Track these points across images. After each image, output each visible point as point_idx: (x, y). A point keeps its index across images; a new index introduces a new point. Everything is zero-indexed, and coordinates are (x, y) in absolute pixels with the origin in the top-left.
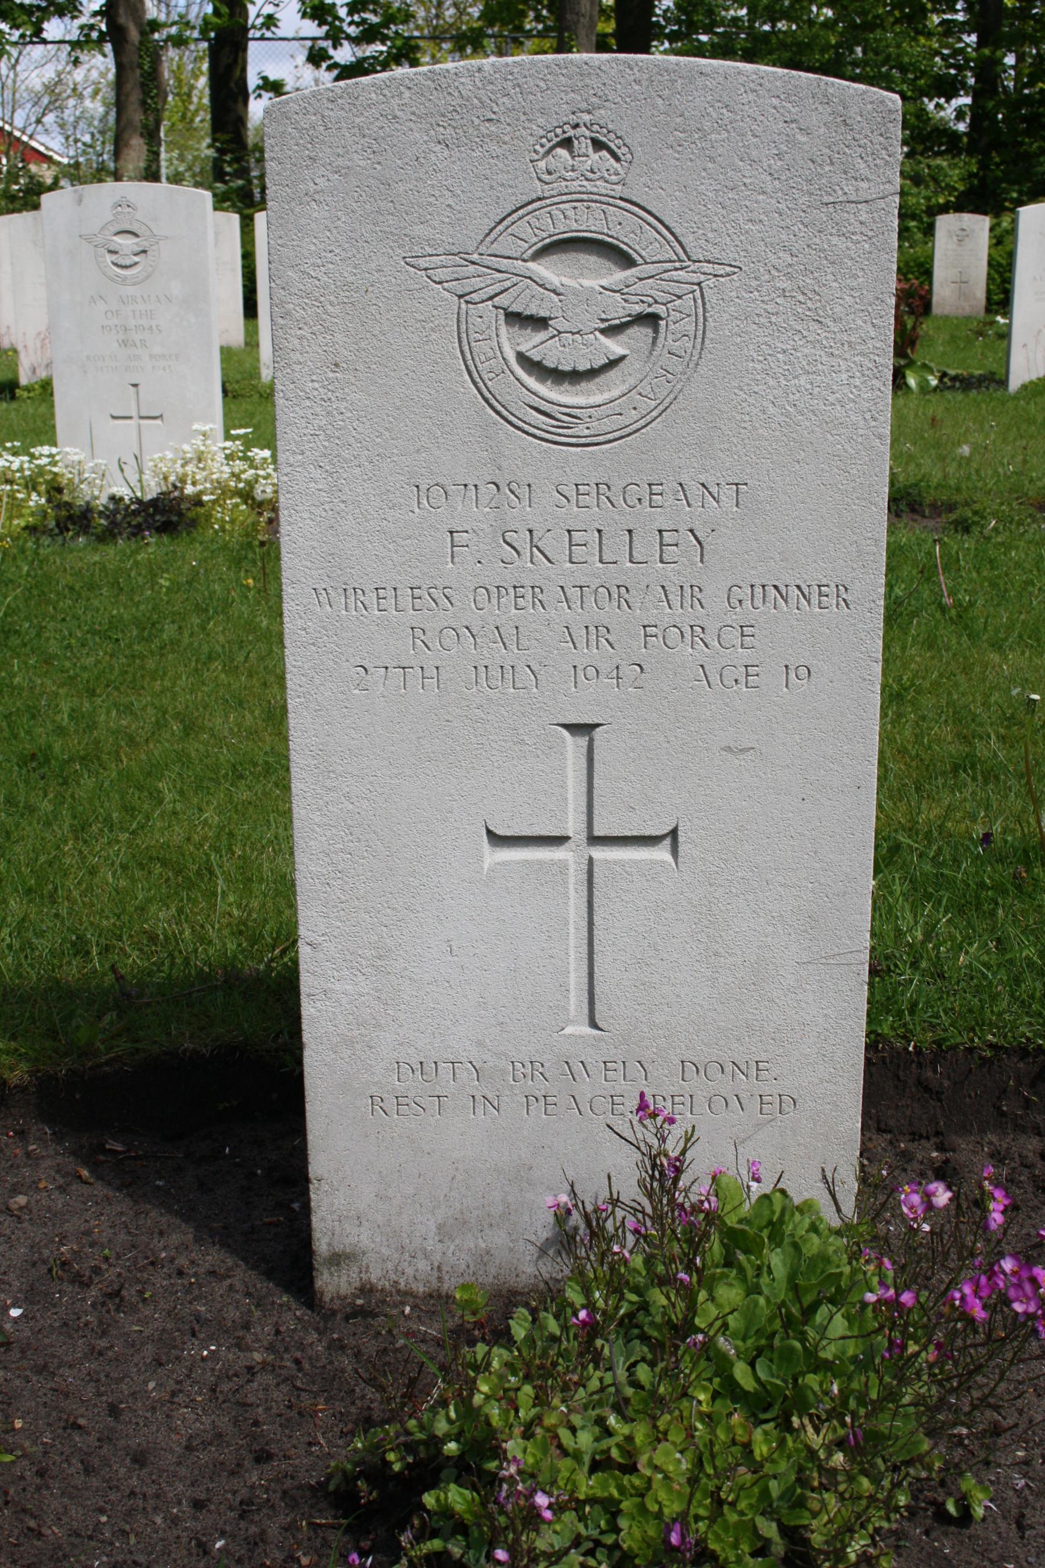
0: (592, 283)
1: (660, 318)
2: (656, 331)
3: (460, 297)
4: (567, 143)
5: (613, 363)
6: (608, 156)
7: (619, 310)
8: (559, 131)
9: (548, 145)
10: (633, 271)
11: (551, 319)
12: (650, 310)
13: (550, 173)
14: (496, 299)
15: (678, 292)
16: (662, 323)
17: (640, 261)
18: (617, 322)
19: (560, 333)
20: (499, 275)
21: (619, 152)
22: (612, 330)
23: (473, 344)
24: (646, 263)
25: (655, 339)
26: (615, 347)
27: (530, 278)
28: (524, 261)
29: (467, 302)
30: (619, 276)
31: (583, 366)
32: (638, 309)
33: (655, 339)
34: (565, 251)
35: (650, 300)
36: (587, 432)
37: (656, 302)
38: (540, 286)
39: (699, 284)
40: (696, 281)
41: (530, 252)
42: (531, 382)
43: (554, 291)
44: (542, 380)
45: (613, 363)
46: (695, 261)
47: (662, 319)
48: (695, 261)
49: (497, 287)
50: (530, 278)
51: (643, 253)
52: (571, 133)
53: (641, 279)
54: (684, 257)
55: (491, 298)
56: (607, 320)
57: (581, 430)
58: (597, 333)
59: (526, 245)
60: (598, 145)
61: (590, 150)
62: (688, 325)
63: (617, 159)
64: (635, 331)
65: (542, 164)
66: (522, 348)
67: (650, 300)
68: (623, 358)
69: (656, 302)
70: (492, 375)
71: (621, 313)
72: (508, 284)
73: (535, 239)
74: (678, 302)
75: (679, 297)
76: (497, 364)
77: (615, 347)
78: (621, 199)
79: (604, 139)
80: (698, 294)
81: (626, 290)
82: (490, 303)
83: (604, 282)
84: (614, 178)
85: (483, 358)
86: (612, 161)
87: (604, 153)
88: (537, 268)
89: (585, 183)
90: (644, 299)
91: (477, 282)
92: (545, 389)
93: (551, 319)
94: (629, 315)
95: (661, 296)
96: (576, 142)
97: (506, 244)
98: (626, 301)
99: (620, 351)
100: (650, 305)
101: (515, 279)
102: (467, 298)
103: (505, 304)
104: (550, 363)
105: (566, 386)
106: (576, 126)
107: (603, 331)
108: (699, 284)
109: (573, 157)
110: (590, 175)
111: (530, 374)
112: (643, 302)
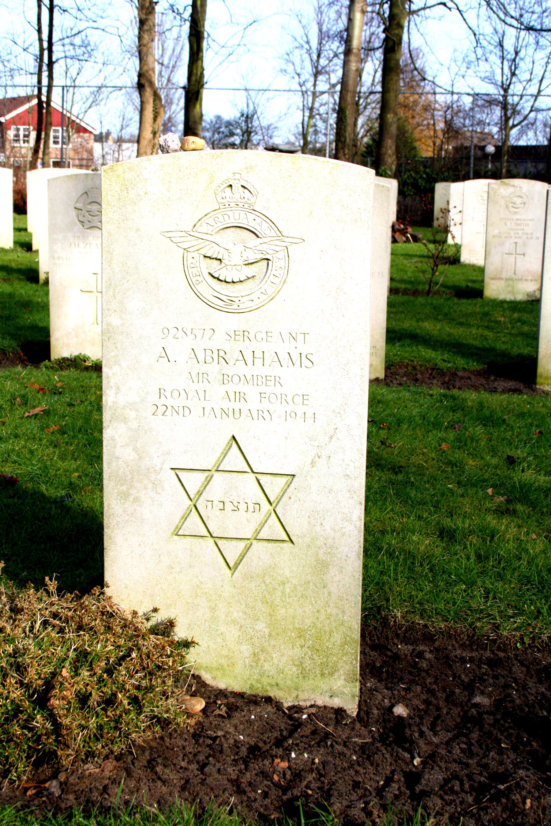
57: (235, 307)
62: (282, 263)
107: (246, 265)
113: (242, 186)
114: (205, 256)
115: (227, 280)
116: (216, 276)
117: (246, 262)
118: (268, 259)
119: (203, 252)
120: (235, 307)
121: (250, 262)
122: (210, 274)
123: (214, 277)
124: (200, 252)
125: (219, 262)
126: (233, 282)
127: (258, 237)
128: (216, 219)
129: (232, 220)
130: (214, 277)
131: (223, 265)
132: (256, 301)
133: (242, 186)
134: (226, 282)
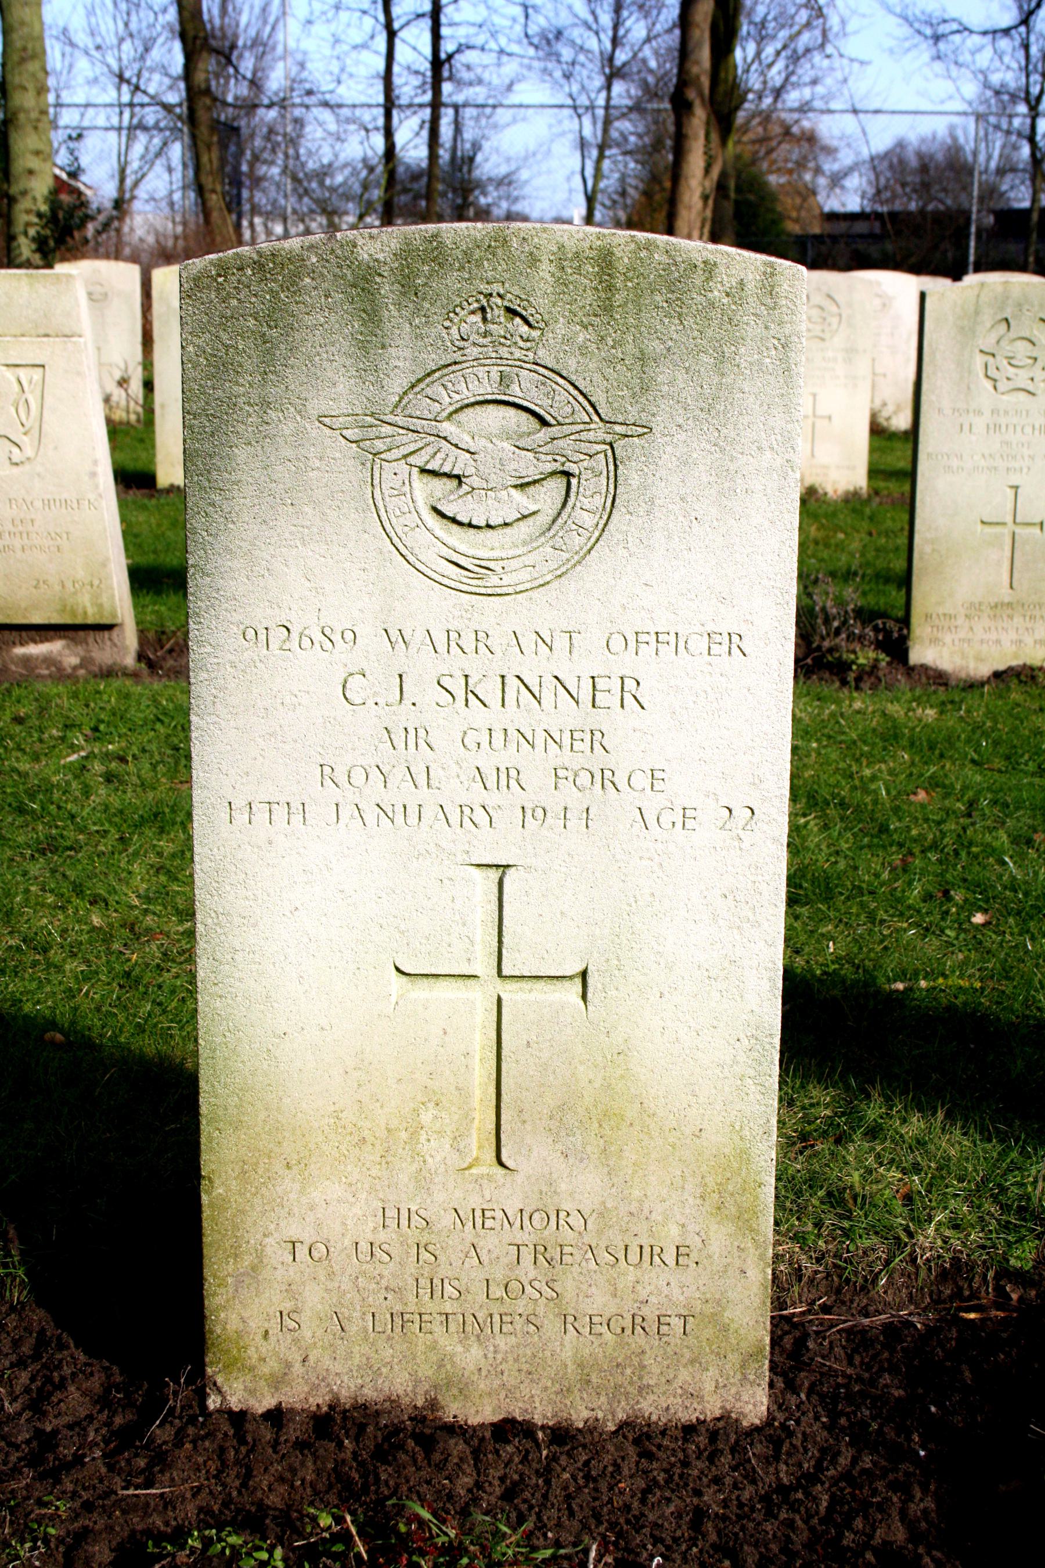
1: (573, 476)
7: (529, 467)
13: (463, 339)
15: (592, 452)
16: (574, 481)
21: (531, 319)
23: (387, 499)
24: (559, 424)
27: (445, 438)
32: (550, 467)
38: (456, 446)
39: (611, 445)
40: (608, 440)
43: (468, 451)
47: (573, 476)
49: (412, 447)
50: (445, 438)
54: (595, 418)
55: (405, 457)
57: (494, 580)
58: (513, 491)
60: (511, 312)
63: (530, 325)
85: (398, 513)
86: (526, 328)
87: (518, 320)
90: (558, 458)
97: (422, 406)
99: (533, 508)
100: (563, 464)
101: (432, 438)
102: (382, 456)
103: (421, 464)
107: (515, 487)
110: (502, 340)
113: (508, 310)
114: (423, 471)
115: (474, 522)
116: (451, 515)
118: (567, 474)
119: (418, 460)
120: (494, 580)
121: (526, 480)
122: (435, 509)
123: (443, 515)
124: (411, 460)
125: (455, 482)
126: (489, 526)
127: (544, 423)
128: (450, 385)
130: (443, 515)
131: (465, 488)
133: (508, 310)
134: (470, 525)
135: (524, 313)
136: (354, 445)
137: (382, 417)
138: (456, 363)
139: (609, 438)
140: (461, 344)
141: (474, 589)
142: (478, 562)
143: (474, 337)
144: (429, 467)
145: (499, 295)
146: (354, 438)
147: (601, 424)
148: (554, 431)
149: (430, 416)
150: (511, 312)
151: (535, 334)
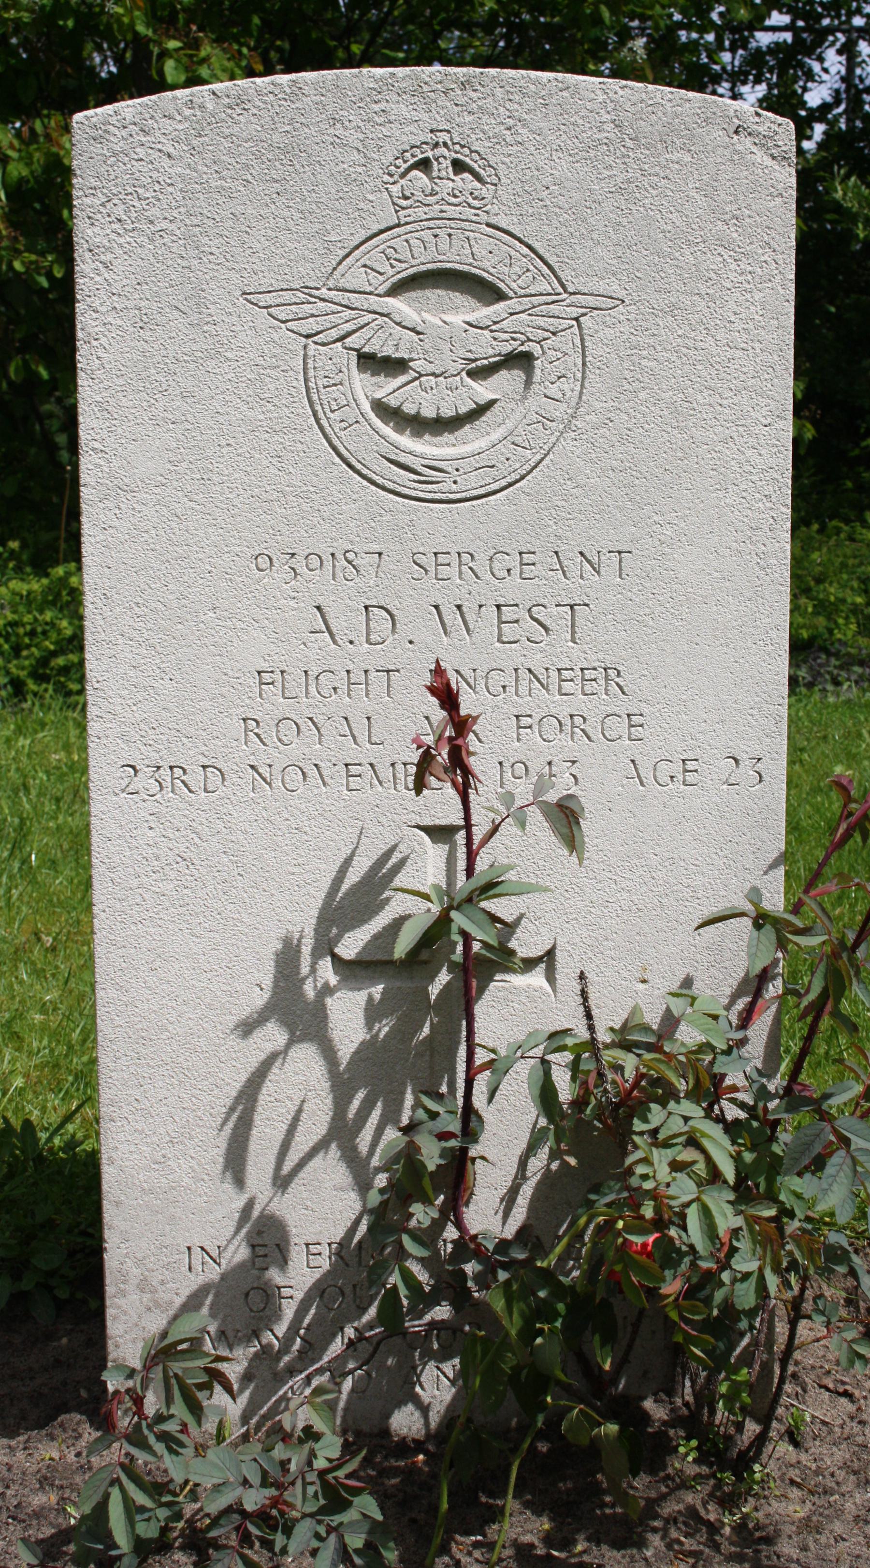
0: (457, 319)
2: (529, 370)
3: (308, 336)
4: (424, 165)
5: (481, 410)
6: (471, 177)
8: (417, 151)
9: (406, 166)
10: (500, 306)
11: (412, 360)
12: (522, 348)
13: (406, 198)
14: (347, 340)
16: (537, 363)
17: (511, 294)
18: (485, 362)
19: (421, 375)
20: (348, 313)
22: (480, 373)
25: (528, 383)
26: (483, 391)
28: (378, 295)
29: (316, 343)
30: (484, 313)
31: (448, 412)
32: (507, 348)
33: (528, 383)
34: (422, 287)
35: (523, 338)
36: (454, 487)
37: (529, 340)
38: (398, 324)
39: (576, 319)
40: (575, 315)
41: (388, 284)
42: (387, 430)
43: (413, 330)
44: (399, 430)
45: (481, 410)
46: (571, 294)
48: (571, 294)
51: (514, 285)
52: (430, 154)
53: (512, 314)
54: (561, 291)
56: (476, 360)
57: (448, 485)
59: (381, 278)
60: (459, 166)
61: (450, 169)
64: (503, 374)
65: (395, 189)
66: (378, 395)
67: (523, 338)
68: (492, 403)
69: (529, 340)
70: (344, 425)
71: (491, 352)
72: (361, 321)
73: (391, 272)
74: (554, 338)
75: (554, 334)
76: (351, 414)
77: (483, 391)
78: (488, 225)
79: (467, 160)
80: (576, 330)
81: (494, 328)
82: (339, 344)
83: (469, 318)
84: (476, 203)
87: (466, 175)
88: (392, 302)
89: (444, 208)
91: (325, 322)
92: (405, 441)
93: (412, 360)
94: (499, 355)
95: (531, 333)
96: (435, 163)
98: (495, 339)
102: (315, 338)
103: (357, 347)
104: (409, 409)
105: (427, 437)
106: (436, 145)
107: (470, 374)
108: (576, 319)
109: (431, 179)
111: (386, 424)
112: (514, 339)
117: (474, 365)
121: (479, 363)
128: (390, 251)
129: (432, 254)
132: (503, 469)
135: (475, 166)
136: (283, 326)
137: (314, 292)
138: (398, 225)
139: (575, 312)
140: (404, 203)
141: (422, 495)
142: (427, 462)
143: (419, 196)
144: (366, 350)
145: (445, 144)
146: (283, 316)
147: (565, 296)
148: (512, 304)
149: (369, 289)
150: (459, 166)
151: (486, 191)
